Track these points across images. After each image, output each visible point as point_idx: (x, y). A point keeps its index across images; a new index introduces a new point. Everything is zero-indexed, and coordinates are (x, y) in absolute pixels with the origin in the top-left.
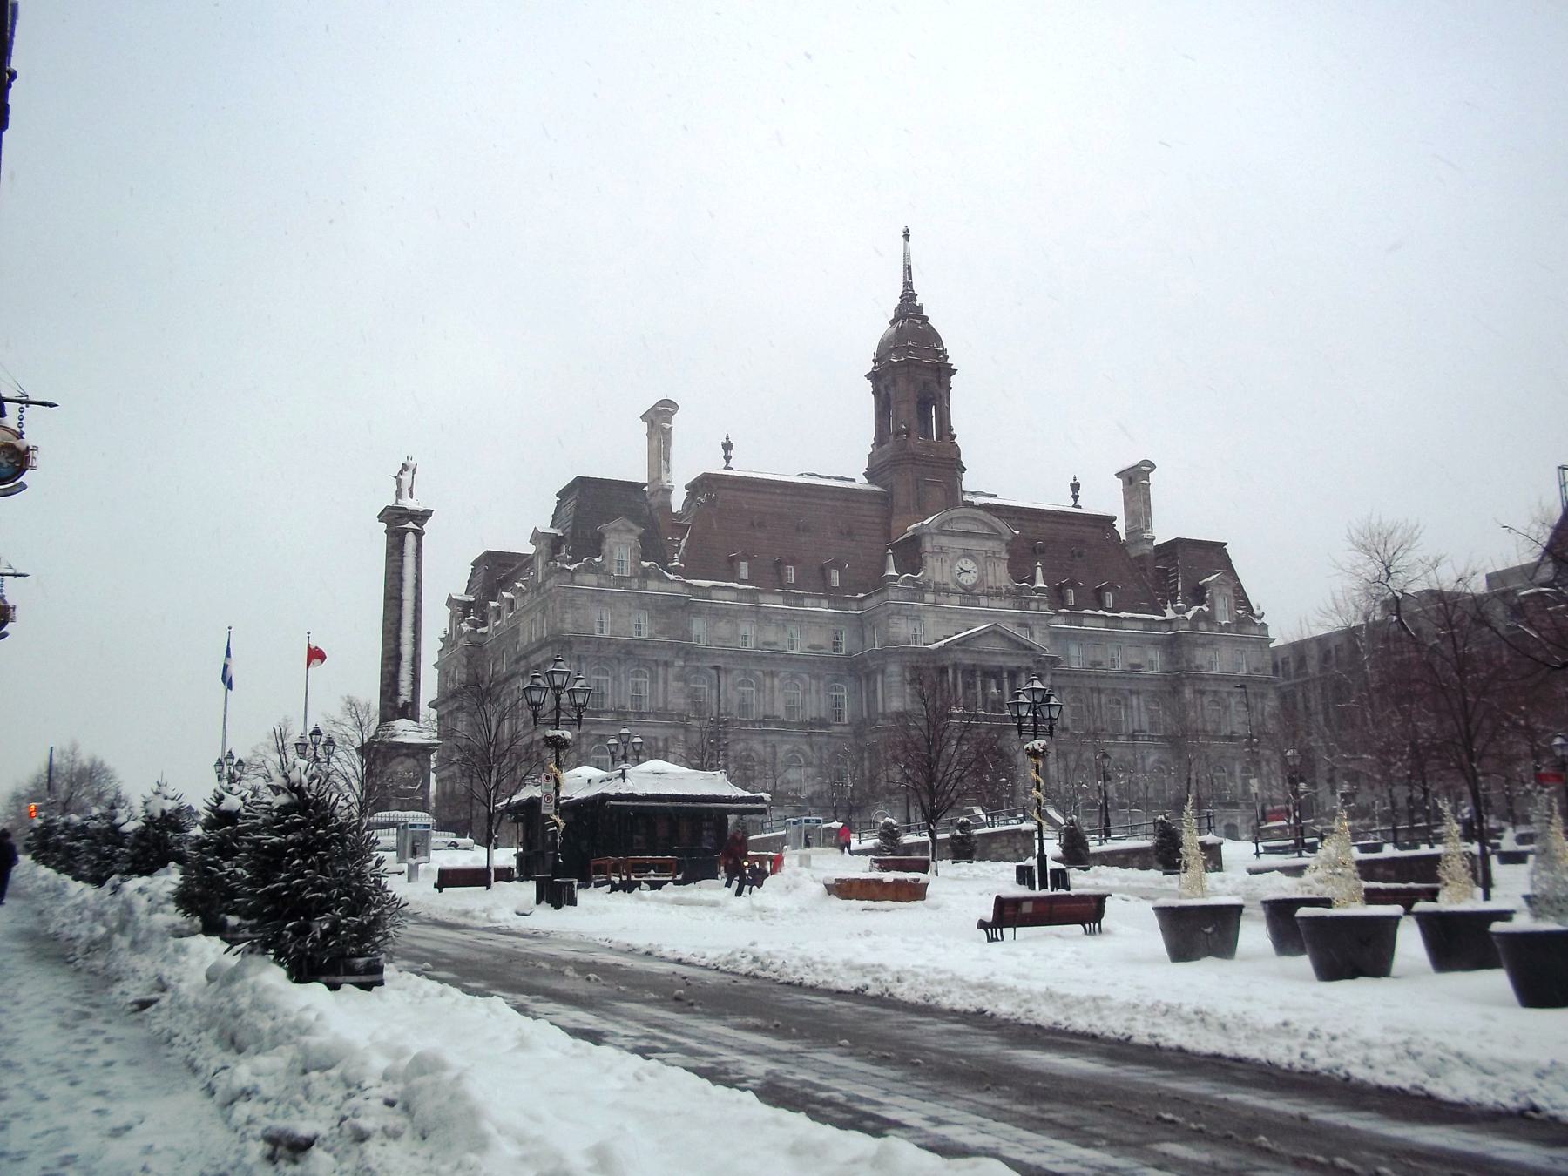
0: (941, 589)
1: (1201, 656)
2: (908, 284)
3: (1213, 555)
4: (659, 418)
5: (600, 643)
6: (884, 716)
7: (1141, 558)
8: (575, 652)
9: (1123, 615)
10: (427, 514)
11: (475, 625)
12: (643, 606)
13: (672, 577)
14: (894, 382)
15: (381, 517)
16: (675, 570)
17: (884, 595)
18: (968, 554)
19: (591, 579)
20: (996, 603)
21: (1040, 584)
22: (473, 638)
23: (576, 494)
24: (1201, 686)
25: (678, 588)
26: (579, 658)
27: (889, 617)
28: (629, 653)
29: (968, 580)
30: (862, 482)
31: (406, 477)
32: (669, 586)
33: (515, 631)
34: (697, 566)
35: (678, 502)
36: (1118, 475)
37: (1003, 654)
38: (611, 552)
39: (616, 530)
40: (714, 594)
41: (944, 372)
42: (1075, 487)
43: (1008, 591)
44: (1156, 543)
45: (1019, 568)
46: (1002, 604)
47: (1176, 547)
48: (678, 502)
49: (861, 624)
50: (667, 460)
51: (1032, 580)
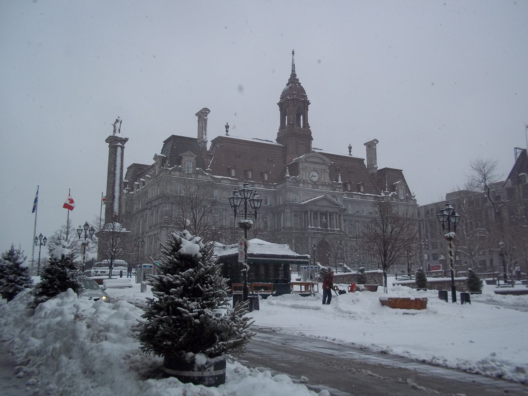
2: (293, 71)
3: (398, 174)
4: (203, 115)
7: (373, 174)
9: (367, 194)
10: (126, 140)
13: (207, 174)
15: (107, 141)
18: (314, 171)
19: (177, 173)
20: (325, 188)
21: (340, 182)
22: (128, 196)
27: (286, 192)
29: (315, 179)
30: (275, 142)
31: (118, 125)
32: (206, 177)
33: (146, 193)
35: (209, 146)
37: (328, 207)
38: (185, 164)
40: (222, 181)
42: (350, 148)
43: (329, 184)
44: (378, 169)
45: (333, 176)
46: (327, 189)
47: (386, 170)
48: (209, 146)
49: (275, 195)
50: (206, 131)
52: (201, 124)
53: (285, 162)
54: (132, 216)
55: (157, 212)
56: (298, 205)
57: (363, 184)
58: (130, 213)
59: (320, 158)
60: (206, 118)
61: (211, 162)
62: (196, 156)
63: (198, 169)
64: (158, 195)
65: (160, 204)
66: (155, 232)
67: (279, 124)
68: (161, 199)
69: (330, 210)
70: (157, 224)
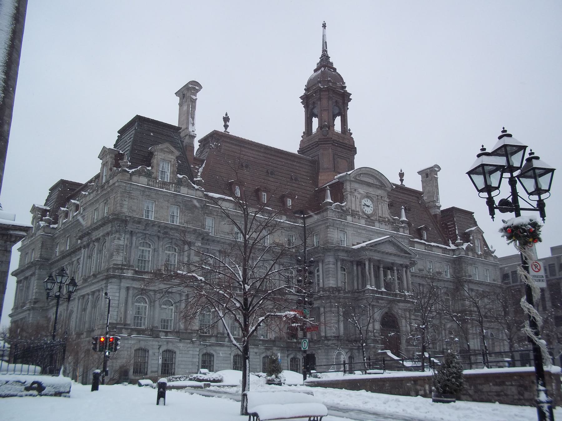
0: (354, 214)
1: (470, 270)
2: (325, 51)
4: (188, 94)
5: (149, 224)
6: (324, 290)
7: (435, 216)
8: (130, 227)
9: (433, 244)
11: (50, 222)
12: (176, 204)
14: (320, 99)
17: (325, 214)
18: (368, 197)
20: (383, 226)
21: (404, 218)
22: (46, 230)
23: (132, 132)
26: (131, 233)
27: (327, 227)
28: (166, 233)
29: (369, 211)
30: (297, 153)
34: (210, 184)
35: (196, 146)
36: (419, 173)
37: (395, 255)
38: (158, 165)
39: (162, 150)
41: (345, 98)
42: (401, 175)
44: (442, 209)
46: (386, 227)
47: (453, 211)
50: (193, 118)
51: (400, 216)
52: (185, 108)
54: (52, 264)
55: (100, 251)
56: (348, 251)
57: (426, 229)
58: (48, 260)
59: (376, 179)
60: (194, 97)
61: (201, 170)
62: (177, 153)
64: (103, 218)
65: (108, 234)
66: (94, 288)
67: (302, 128)
68: (110, 225)
69: (399, 261)
70: (99, 273)
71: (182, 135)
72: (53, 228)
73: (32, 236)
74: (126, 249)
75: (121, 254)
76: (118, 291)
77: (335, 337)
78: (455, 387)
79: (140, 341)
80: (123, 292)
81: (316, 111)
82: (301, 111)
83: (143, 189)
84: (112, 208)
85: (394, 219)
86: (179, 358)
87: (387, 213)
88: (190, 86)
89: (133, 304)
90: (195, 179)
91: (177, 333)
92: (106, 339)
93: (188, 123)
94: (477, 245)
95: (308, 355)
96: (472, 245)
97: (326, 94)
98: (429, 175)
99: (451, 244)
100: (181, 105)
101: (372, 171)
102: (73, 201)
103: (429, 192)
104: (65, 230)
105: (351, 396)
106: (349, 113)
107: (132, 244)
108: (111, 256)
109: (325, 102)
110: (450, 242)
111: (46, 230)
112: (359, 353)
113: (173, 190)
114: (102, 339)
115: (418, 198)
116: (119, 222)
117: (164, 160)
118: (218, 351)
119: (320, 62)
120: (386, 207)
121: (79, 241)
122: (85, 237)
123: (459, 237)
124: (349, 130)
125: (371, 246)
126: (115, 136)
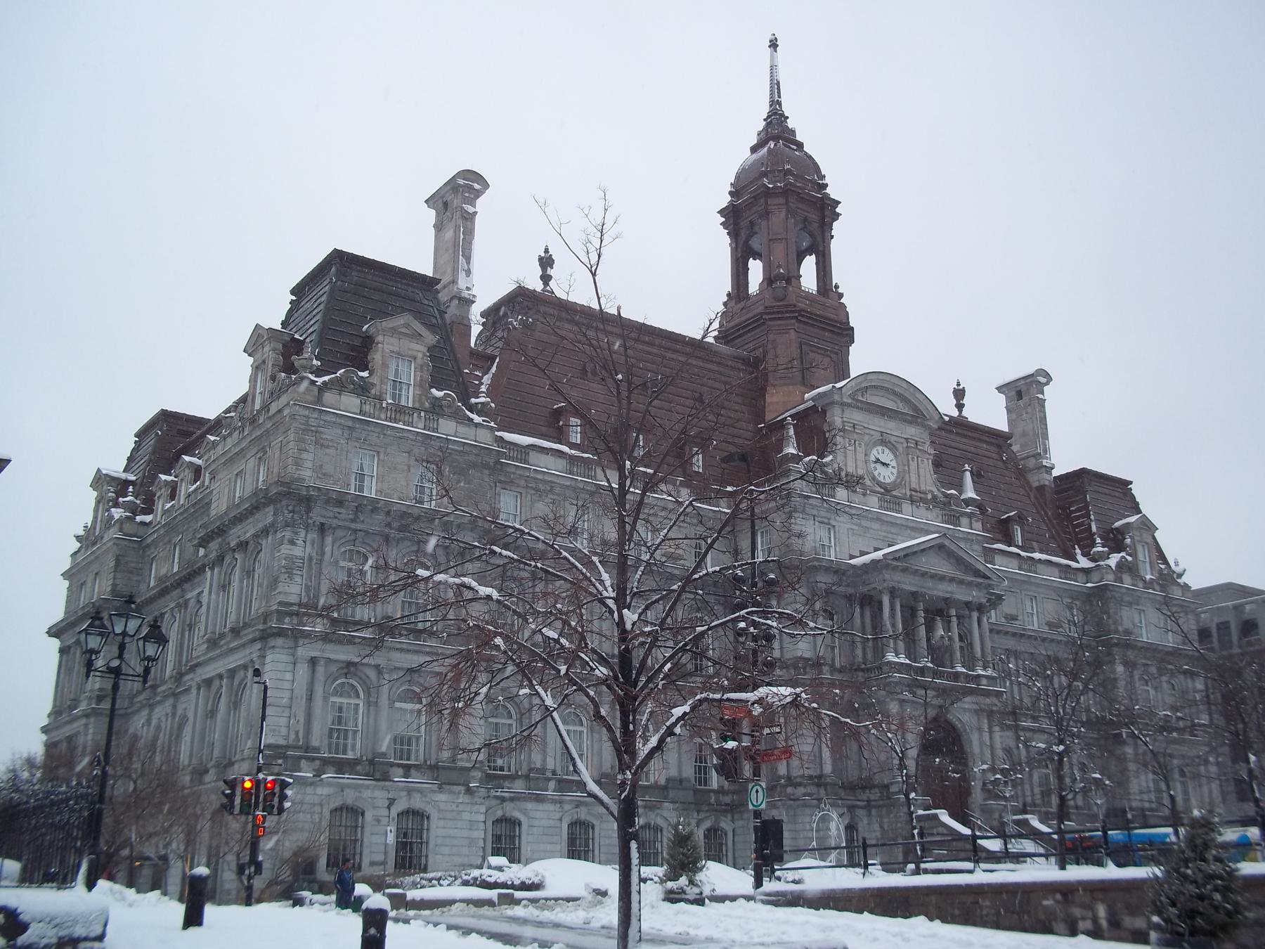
0: (852, 483)
2: (775, 103)
4: (456, 200)
5: (362, 506)
7: (1041, 489)
8: (317, 516)
9: (1037, 555)
11: (134, 510)
14: (766, 214)
16: (481, 410)
18: (884, 442)
21: (970, 493)
22: (128, 527)
24: (1131, 655)
25: (484, 438)
29: (887, 475)
32: (475, 432)
33: (202, 505)
36: (999, 389)
37: (952, 580)
38: (385, 366)
39: (394, 331)
40: (533, 457)
42: (959, 394)
43: (934, 497)
44: (1055, 473)
50: (468, 259)
51: (960, 487)
52: (449, 234)
53: (759, 414)
55: (249, 573)
56: (839, 571)
57: (1021, 519)
59: (906, 401)
60: (470, 209)
61: (487, 379)
62: (431, 338)
63: (439, 394)
65: (265, 532)
67: (725, 285)
69: (962, 594)
70: (246, 625)
71: (443, 296)
72: (143, 523)
73: (94, 544)
74: (310, 567)
75: (298, 579)
76: (290, 667)
77: (811, 777)
78: (1220, 917)
79: (342, 788)
80: (303, 670)
81: (755, 244)
82: (721, 244)
83: (350, 423)
84: (276, 470)
85: (946, 496)
86: (437, 830)
87: (930, 481)
88: (461, 182)
89: (325, 699)
90: (473, 400)
91: (434, 769)
92: (257, 783)
93: (455, 271)
94: (1141, 557)
95: (764, 823)
96: (1129, 558)
97: (781, 202)
98: (1025, 393)
99: (1079, 557)
100: (439, 227)
101: (895, 381)
102: (187, 458)
103: (1024, 434)
104: (171, 528)
105: (906, 940)
106: (836, 247)
107: (323, 554)
108: (274, 583)
109: (778, 218)
110: (1078, 551)
111: (128, 527)
112: (869, 815)
113: (421, 425)
114: (248, 785)
115: (999, 446)
116: (291, 501)
117: (399, 355)
118: (532, 814)
119: (766, 128)
120: (927, 467)
121: (202, 552)
122: (213, 539)
123: (1098, 540)
124: (837, 287)
125: (895, 559)
126: (284, 302)
